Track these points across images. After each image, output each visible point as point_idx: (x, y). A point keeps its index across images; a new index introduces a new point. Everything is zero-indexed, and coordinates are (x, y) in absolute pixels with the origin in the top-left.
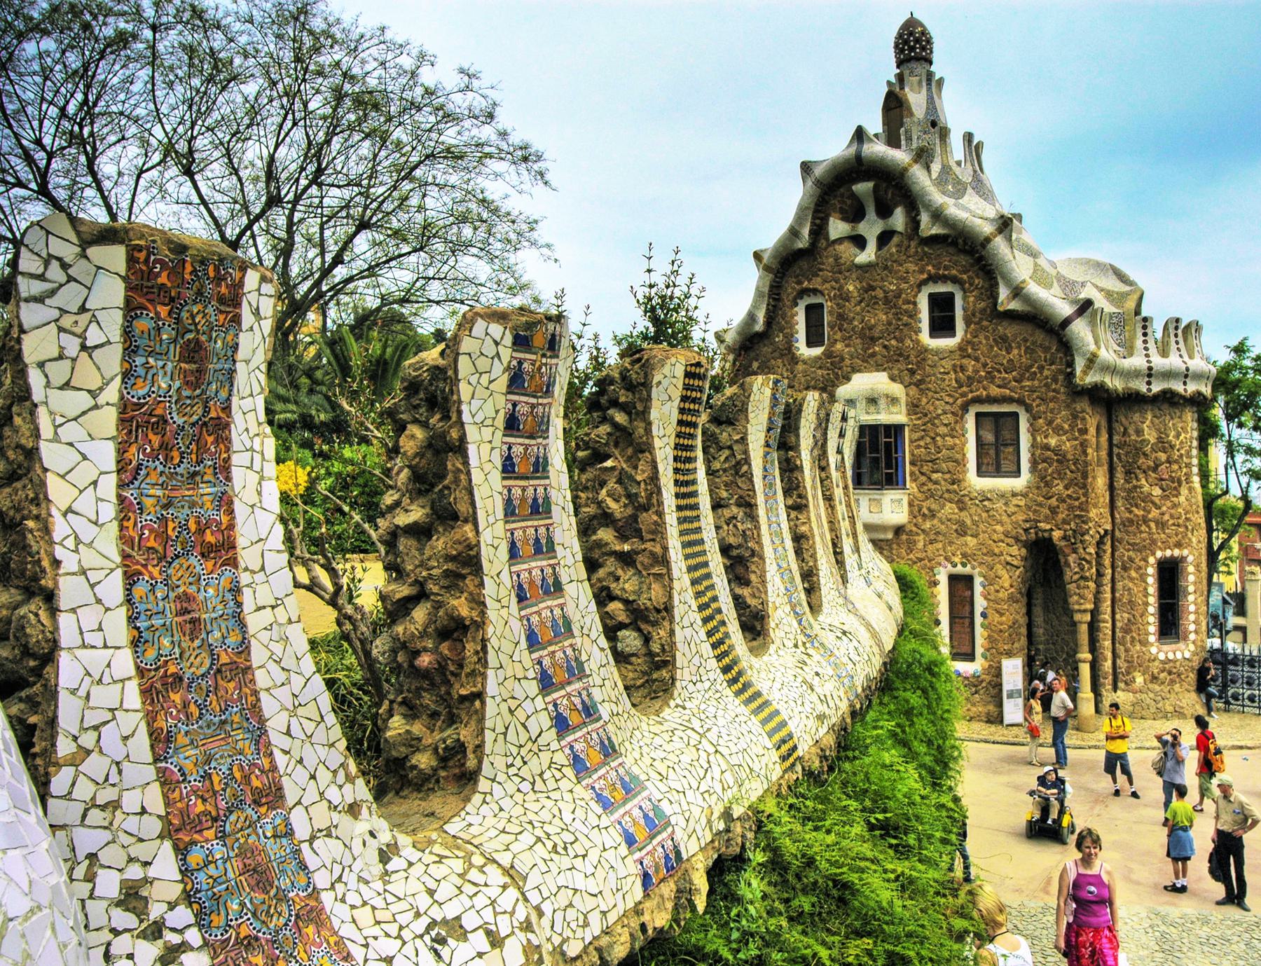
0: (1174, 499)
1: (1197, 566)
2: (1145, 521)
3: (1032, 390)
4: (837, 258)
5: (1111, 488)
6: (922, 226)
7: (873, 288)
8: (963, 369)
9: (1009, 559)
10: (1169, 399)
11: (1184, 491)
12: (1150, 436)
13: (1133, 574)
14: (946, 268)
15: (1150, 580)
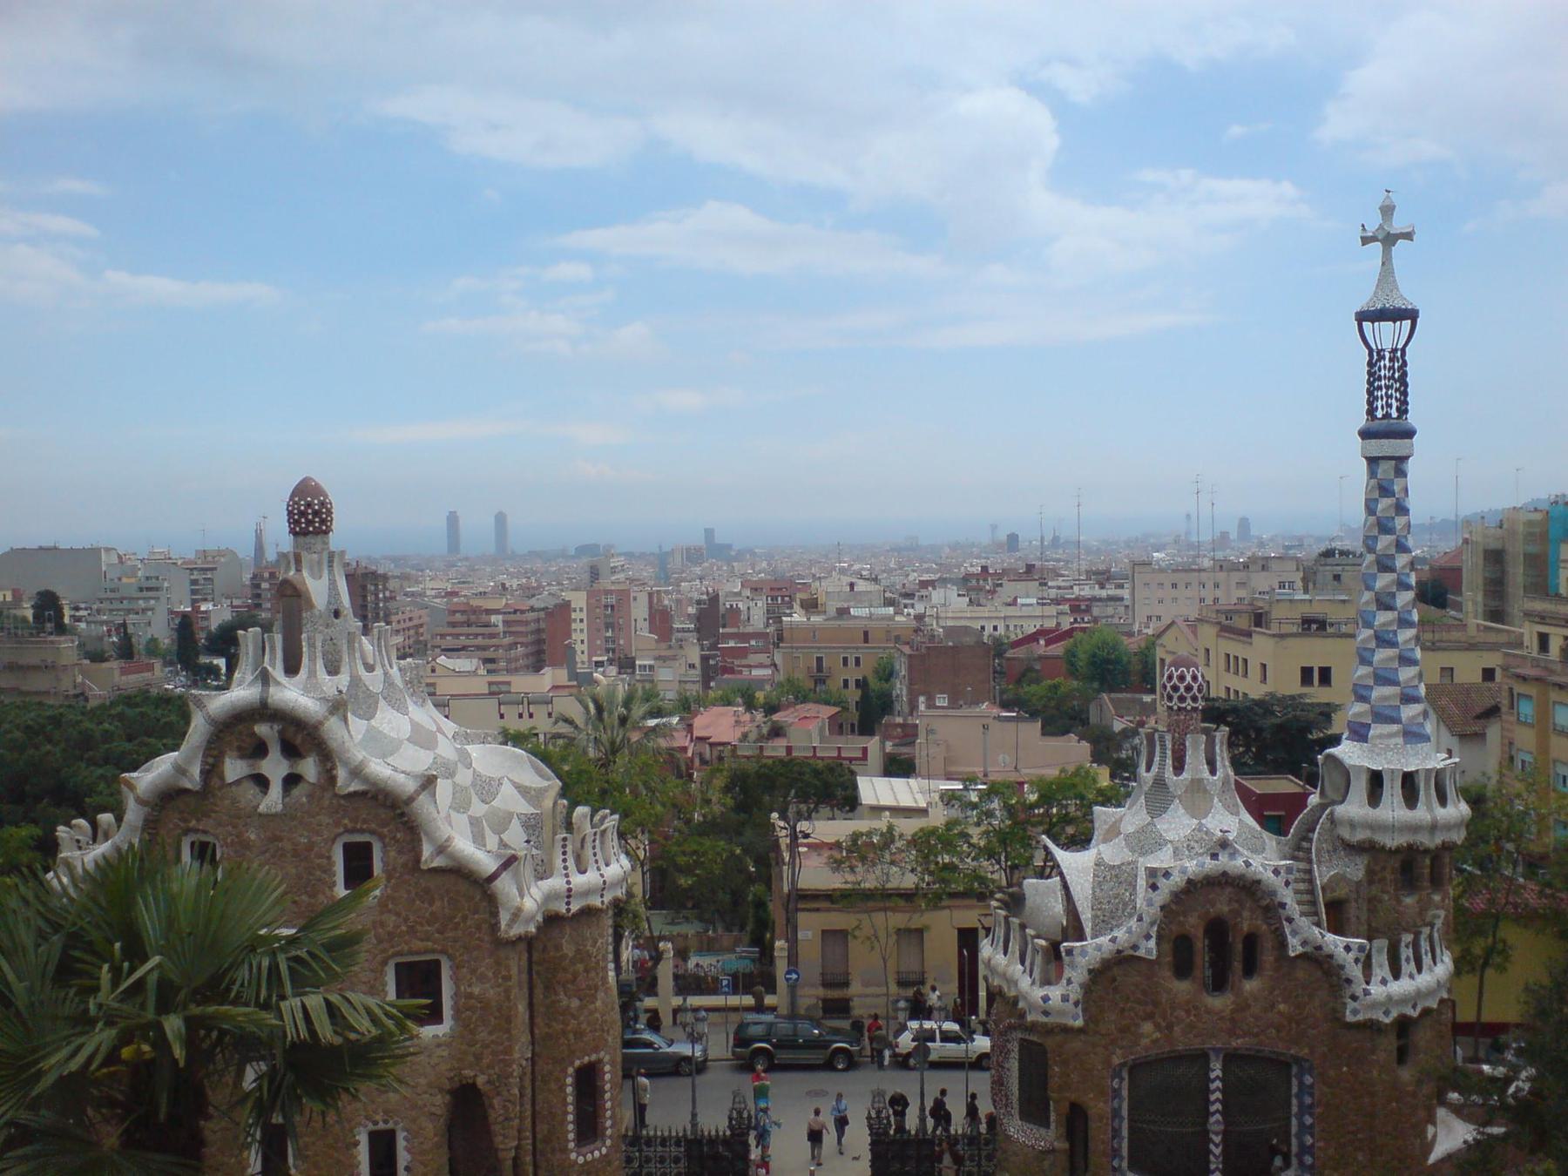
0: (592, 1007)
1: (612, 1063)
2: (564, 1033)
3: (455, 940)
4: (234, 801)
5: (531, 1005)
6: (339, 783)
7: (280, 839)
8: (382, 924)
9: (433, 1109)
10: (588, 913)
11: (601, 995)
12: (568, 949)
13: (553, 1086)
14: (365, 821)
15: (569, 1090)
